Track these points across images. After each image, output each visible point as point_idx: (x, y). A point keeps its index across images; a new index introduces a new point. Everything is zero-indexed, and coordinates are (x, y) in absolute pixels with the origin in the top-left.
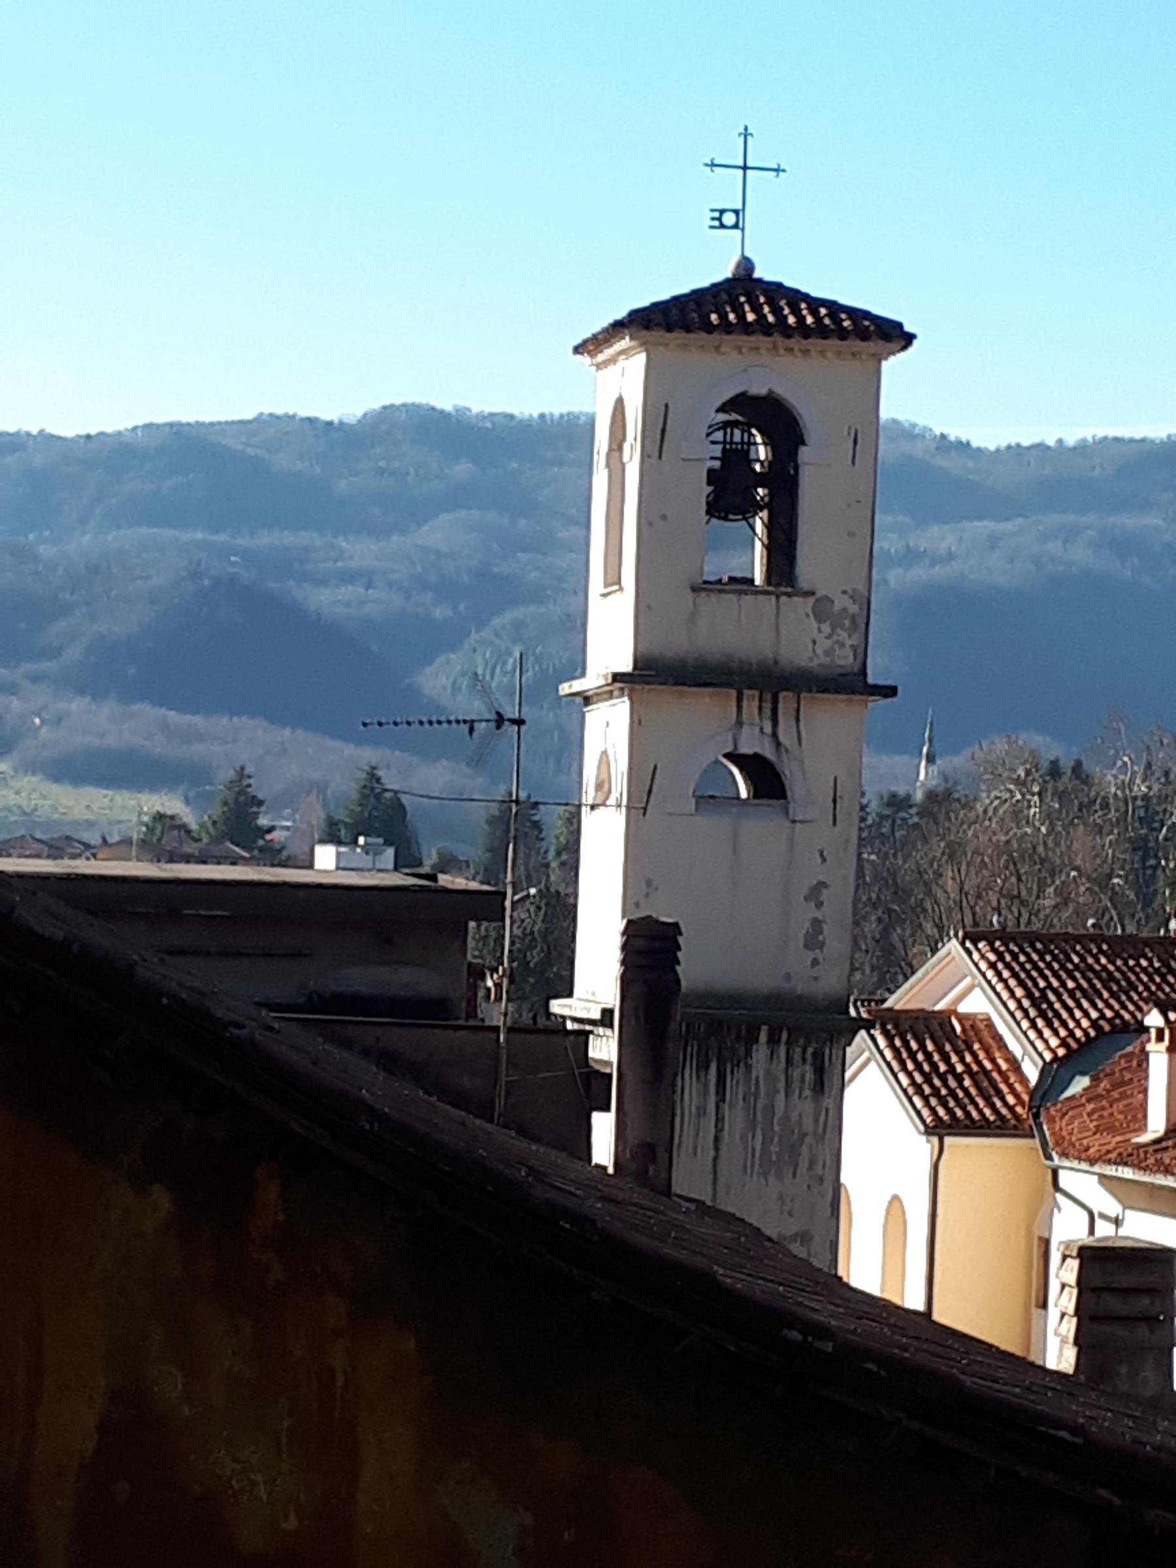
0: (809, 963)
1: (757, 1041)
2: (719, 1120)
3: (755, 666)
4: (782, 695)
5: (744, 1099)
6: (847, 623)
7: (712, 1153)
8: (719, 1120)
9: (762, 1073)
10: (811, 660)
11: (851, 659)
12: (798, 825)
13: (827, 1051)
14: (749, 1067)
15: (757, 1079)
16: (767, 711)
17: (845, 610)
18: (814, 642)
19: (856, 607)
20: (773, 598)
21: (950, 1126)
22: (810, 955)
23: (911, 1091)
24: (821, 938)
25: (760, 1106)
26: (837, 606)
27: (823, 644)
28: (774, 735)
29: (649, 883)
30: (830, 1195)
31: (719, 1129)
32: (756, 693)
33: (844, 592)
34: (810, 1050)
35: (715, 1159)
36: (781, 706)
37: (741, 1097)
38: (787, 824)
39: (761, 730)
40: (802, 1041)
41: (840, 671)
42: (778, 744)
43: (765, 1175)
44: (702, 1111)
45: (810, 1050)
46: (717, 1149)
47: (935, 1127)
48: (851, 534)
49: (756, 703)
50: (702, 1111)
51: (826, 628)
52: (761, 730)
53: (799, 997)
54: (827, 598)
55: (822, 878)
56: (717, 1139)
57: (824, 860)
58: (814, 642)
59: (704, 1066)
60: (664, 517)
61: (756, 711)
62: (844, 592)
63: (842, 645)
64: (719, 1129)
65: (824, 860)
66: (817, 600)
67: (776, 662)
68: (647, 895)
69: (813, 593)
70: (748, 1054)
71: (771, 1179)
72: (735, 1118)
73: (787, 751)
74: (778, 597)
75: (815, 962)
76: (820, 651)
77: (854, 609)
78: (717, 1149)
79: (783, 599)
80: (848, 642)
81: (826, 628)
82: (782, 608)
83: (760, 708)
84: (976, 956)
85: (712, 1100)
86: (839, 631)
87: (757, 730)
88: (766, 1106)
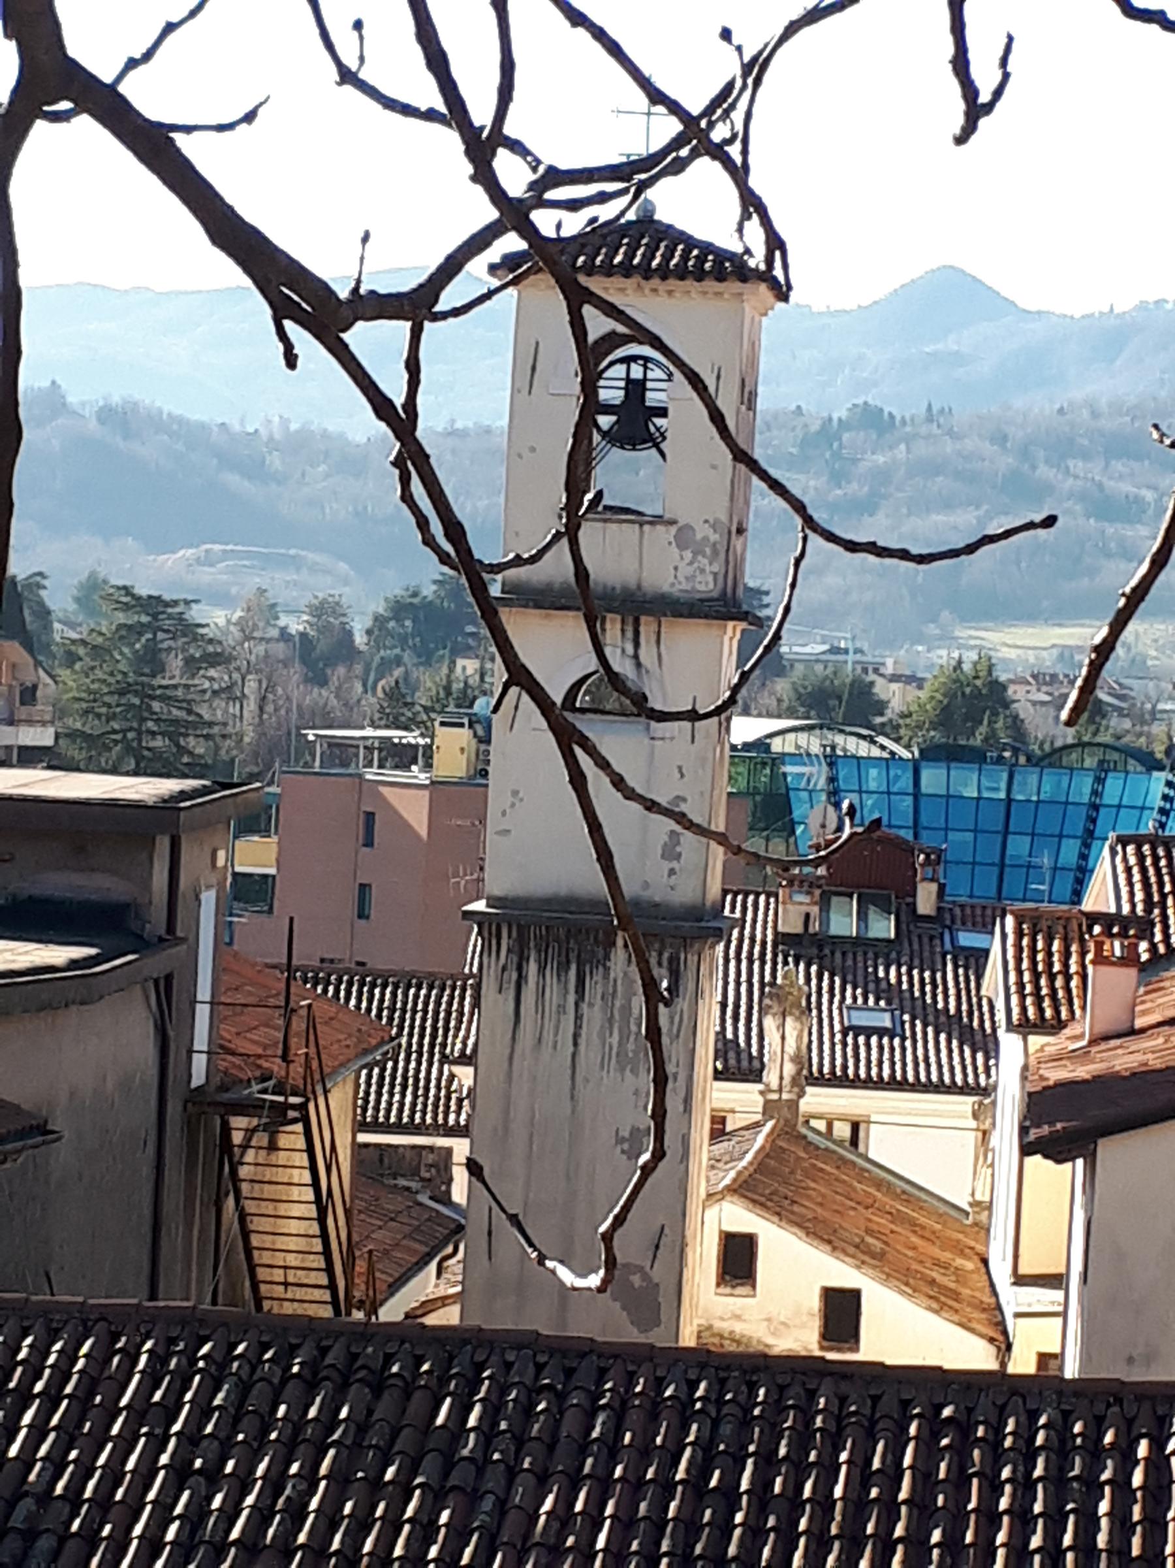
0: (666, 873)
1: (614, 944)
2: (578, 1017)
3: (618, 591)
4: (643, 619)
5: (603, 998)
6: (708, 551)
7: (571, 1049)
8: (578, 1017)
9: (621, 975)
10: (673, 585)
11: (711, 586)
12: (658, 743)
13: (682, 956)
14: (607, 969)
15: (615, 981)
16: (630, 634)
17: (705, 539)
18: (676, 568)
19: (717, 536)
20: (637, 526)
21: (1035, 1025)
22: (666, 865)
23: (1013, 989)
24: (678, 849)
25: (618, 1004)
26: (699, 536)
27: (685, 570)
28: (636, 657)
29: (515, 793)
30: (682, 1094)
31: (578, 1027)
32: (619, 617)
33: (706, 521)
34: (666, 955)
35: (574, 1055)
36: (642, 629)
37: (599, 997)
38: (646, 741)
39: (623, 651)
40: (657, 946)
41: (698, 596)
42: (639, 665)
43: (622, 1070)
44: (562, 1009)
45: (666, 955)
46: (576, 1044)
47: (1020, 1025)
48: (714, 467)
49: (619, 626)
50: (562, 1009)
51: (688, 555)
52: (623, 651)
53: (657, 905)
54: (688, 527)
55: (681, 794)
56: (576, 1037)
57: (682, 776)
58: (676, 568)
59: (563, 967)
60: (533, 450)
61: (619, 633)
62: (706, 521)
63: (702, 571)
64: (578, 1027)
65: (682, 776)
66: (680, 530)
67: (639, 587)
68: (513, 805)
69: (672, 522)
70: (607, 957)
71: (628, 1072)
72: (594, 1015)
73: (647, 672)
74: (641, 525)
75: (672, 872)
76: (681, 578)
77: (714, 537)
78: (576, 1044)
79: (646, 528)
80: (708, 568)
81: (688, 555)
82: (646, 536)
83: (623, 631)
84: (1119, 859)
85: (572, 998)
86: (700, 558)
87: (619, 651)
88: (622, 1006)
